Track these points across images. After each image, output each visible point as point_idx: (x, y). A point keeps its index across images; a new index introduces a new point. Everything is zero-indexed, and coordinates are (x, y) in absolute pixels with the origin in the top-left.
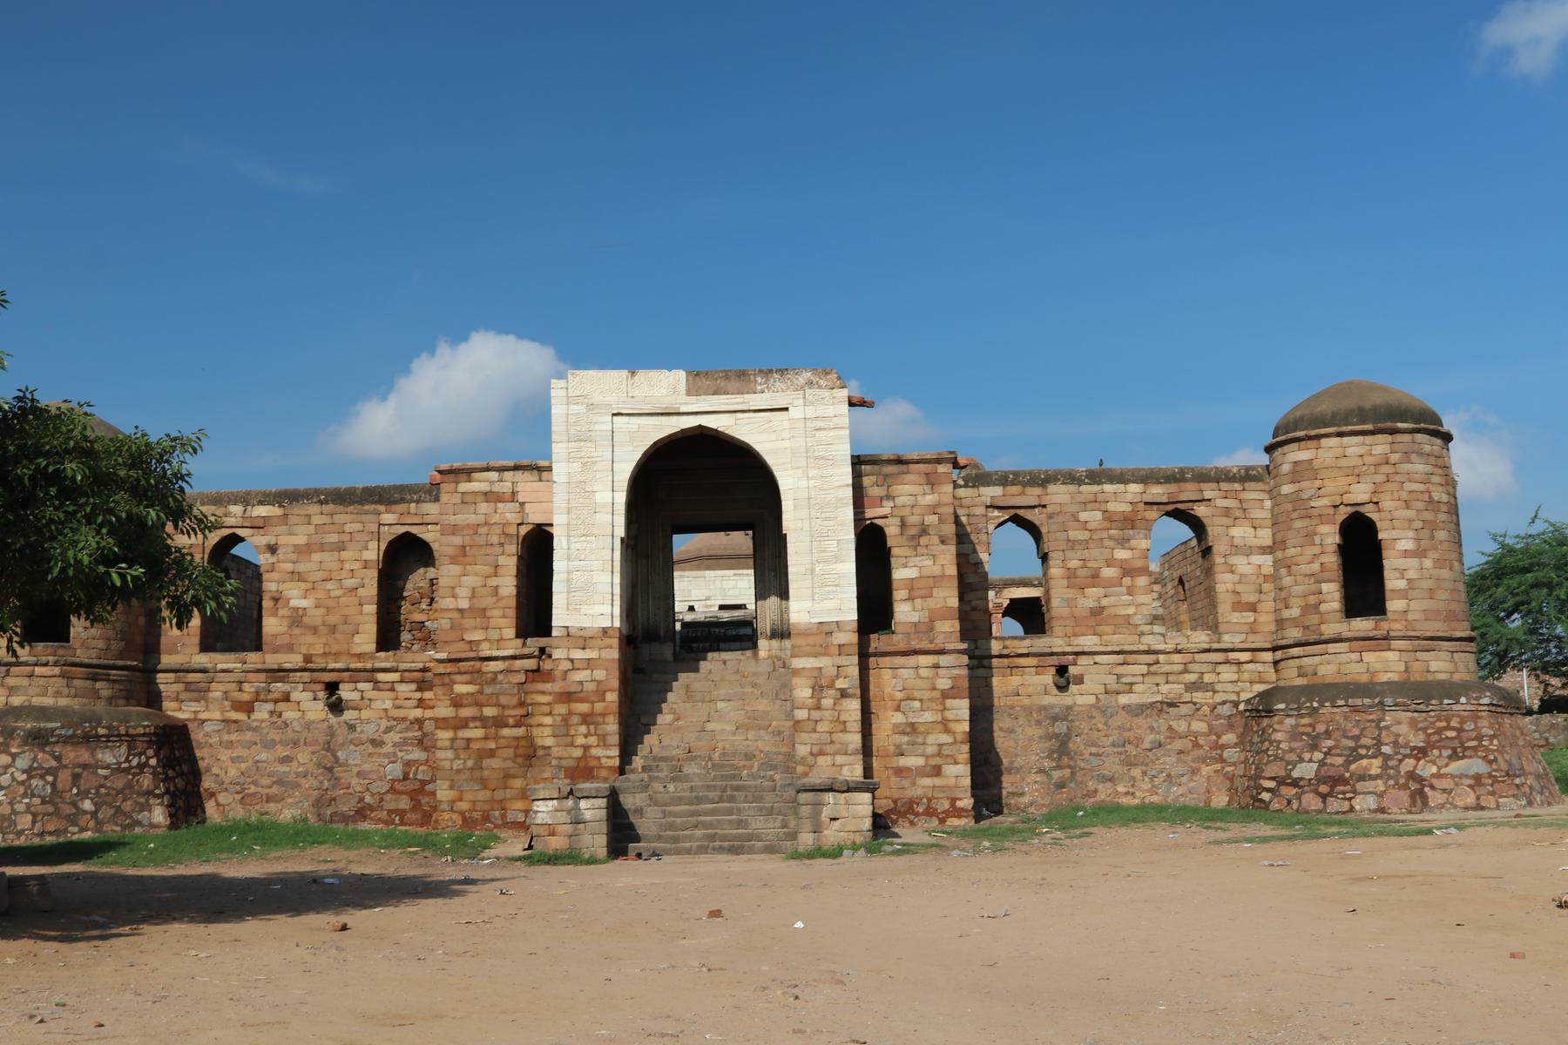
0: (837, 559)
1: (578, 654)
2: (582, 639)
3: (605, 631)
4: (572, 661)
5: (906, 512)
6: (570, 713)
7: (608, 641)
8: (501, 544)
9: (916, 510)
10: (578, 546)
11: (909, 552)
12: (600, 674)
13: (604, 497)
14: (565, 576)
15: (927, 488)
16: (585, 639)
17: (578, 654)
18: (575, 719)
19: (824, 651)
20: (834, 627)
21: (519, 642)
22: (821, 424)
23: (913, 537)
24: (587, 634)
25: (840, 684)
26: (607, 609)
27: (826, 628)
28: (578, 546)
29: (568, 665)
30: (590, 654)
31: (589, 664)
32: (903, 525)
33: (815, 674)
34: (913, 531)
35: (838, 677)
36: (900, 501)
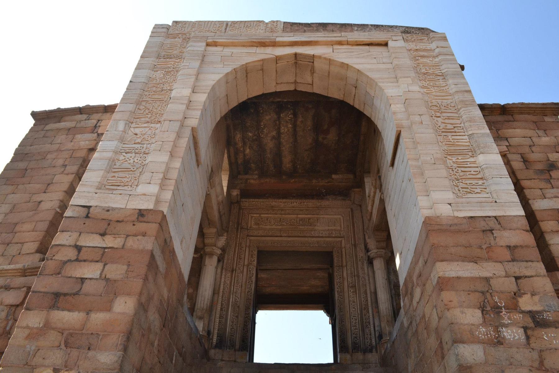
1: (92, 241)
2: (104, 222)
3: (141, 214)
4: (79, 248)
5: (526, 150)
6: (47, 326)
7: (141, 227)
8: (65, 166)
9: (534, 149)
10: (137, 131)
11: (542, 185)
12: (116, 271)
13: (181, 90)
14: (109, 155)
15: (541, 133)
17: (92, 241)
18: (53, 337)
19: (486, 254)
20: (492, 224)
21: (38, 256)
22: (426, 54)
23: (541, 171)
24: (114, 216)
25: (527, 303)
28: (137, 131)
29: (72, 254)
30: (109, 242)
31: (103, 256)
32: (525, 161)
33: (480, 286)
34: (540, 166)
35: (517, 294)
36: (514, 141)
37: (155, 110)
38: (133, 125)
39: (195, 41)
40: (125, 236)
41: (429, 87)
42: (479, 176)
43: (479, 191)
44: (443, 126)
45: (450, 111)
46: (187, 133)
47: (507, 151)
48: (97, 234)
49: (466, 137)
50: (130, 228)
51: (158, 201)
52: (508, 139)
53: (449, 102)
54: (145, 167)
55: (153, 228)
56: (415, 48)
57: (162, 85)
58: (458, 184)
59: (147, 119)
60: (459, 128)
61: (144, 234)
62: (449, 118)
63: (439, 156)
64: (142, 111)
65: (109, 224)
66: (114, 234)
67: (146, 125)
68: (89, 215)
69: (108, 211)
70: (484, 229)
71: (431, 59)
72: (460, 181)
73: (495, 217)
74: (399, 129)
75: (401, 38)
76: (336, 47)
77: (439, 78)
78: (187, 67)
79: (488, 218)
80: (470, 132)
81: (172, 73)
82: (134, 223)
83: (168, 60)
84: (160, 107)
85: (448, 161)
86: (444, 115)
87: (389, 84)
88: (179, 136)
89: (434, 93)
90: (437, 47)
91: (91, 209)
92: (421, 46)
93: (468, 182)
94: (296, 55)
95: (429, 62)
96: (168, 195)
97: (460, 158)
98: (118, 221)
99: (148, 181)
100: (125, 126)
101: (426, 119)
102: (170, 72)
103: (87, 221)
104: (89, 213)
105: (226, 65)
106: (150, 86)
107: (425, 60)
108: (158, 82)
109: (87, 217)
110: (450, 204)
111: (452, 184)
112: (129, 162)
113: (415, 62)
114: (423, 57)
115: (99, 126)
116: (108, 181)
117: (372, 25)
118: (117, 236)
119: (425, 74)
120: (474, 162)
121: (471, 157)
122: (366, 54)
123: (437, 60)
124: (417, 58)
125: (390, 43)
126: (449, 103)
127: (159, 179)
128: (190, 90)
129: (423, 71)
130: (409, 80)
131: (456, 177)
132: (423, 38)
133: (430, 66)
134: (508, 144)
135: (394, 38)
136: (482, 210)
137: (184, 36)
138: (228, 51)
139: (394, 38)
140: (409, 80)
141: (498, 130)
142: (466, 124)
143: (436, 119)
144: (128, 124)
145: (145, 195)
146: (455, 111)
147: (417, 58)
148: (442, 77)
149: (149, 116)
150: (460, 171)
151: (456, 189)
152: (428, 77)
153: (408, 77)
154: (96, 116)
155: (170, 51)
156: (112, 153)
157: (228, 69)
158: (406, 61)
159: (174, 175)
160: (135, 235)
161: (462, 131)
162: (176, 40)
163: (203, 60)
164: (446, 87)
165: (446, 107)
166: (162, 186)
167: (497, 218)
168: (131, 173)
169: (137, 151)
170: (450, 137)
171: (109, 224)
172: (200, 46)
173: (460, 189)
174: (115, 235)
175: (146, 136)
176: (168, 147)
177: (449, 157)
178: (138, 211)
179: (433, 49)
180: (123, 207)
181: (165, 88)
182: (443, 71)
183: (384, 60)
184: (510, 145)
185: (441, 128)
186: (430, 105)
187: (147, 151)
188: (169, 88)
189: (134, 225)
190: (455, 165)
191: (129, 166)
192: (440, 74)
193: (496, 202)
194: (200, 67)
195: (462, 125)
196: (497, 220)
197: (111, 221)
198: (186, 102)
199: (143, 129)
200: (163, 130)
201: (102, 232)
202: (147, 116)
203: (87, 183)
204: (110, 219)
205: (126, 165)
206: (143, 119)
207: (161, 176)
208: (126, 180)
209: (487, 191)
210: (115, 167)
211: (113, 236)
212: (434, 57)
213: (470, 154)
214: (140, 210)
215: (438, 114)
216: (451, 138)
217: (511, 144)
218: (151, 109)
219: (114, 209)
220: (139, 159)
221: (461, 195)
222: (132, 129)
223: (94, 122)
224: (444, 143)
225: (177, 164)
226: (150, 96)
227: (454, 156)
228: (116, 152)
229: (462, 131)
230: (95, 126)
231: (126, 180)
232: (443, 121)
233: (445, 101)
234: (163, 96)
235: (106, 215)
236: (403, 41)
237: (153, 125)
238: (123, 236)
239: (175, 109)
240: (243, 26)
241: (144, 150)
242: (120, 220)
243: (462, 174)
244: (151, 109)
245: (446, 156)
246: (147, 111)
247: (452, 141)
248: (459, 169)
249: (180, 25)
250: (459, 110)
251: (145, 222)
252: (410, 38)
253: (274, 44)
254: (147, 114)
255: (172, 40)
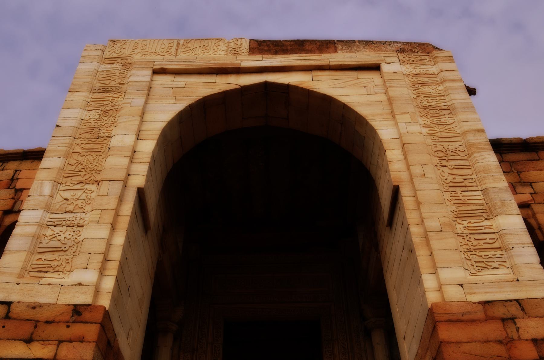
0: (489, 212)
3: (77, 310)
7: (78, 329)
10: (67, 195)
13: (122, 138)
14: (32, 230)
16: (36, 323)
20: (514, 310)
22: (427, 80)
24: (43, 315)
26: (90, 277)
27: (500, 312)
28: (67, 195)
37: (90, 166)
38: (62, 187)
39: (138, 69)
40: (57, 342)
41: (432, 125)
42: (497, 245)
43: (496, 265)
44: (450, 178)
45: (459, 157)
46: (131, 196)
47: (531, 201)
48: (20, 340)
49: (479, 193)
50: (63, 332)
51: (97, 292)
52: (533, 184)
53: (457, 144)
54: (79, 245)
55: (91, 331)
56: (414, 72)
57: (97, 130)
58: (471, 256)
59: (79, 178)
60: (470, 181)
61: (81, 340)
62: (457, 167)
63: (446, 220)
64: (74, 167)
65: (36, 327)
66: (43, 341)
67: (78, 187)
68: (10, 315)
69: (34, 308)
70: (505, 316)
71: (434, 87)
72: (473, 253)
73: (517, 301)
74: (396, 184)
75: (396, 59)
76: (316, 73)
77: (444, 112)
78: (129, 105)
79: (509, 303)
80: (484, 187)
81: (110, 112)
82: (68, 324)
83: (104, 94)
84: (96, 161)
85: (458, 226)
86: (453, 163)
87: (382, 122)
88: (121, 200)
89: (439, 134)
90: (442, 71)
91: (12, 306)
92: (421, 69)
93: (483, 253)
94: (266, 85)
95: (431, 91)
96: (109, 283)
97: (472, 221)
98: (47, 322)
99: (85, 266)
100: (52, 189)
101: (430, 171)
102: (106, 112)
103: (8, 323)
104: (9, 312)
105: (178, 100)
106: (82, 132)
107: (426, 89)
108: (92, 126)
109: (7, 317)
110: (461, 285)
111: (463, 256)
112: (59, 238)
113: (414, 92)
114: (424, 84)
115: (18, 179)
116: (33, 266)
117: (359, 42)
118: (47, 342)
119: (426, 107)
120: (489, 227)
121: (486, 219)
122: (352, 82)
123: (441, 88)
124: (417, 86)
125: (385, 68)
126: (457, 146)
127: (97, 262)
128: (134, 137)
129: (425, 103)
130: (407, 118)
131: (468, 247)
132: (423, 58)
133: (433, 96)
134: (532, 191)
135: (388, 60)
136: (500, 292)
137: (124, 61)
138: (180, 81)
139: (388, 60)
140: (407, 118)
141: (519, 173)
142: (479, 175)
143: (442, 168)
144: (57, 186)
145: (80, 284)
146: (465, 158)
147: (417, 86)
148: (449, 112)
149: (82, 174)
150: (472, 239)
151: (469, 263)
152: (431, 112)
153: (405, 113)
154: (12, 165)
155: (107, 82)
156: (36, 227)
157: (180, 107)
158: (402, 91)
159: (116, 254)
160: (70, 341)
161: (474, 184)
162: (114, 66)
163: (148, 94)
164: (454, 125)
165: (455, 152)
166: (102, 272)
167: (520, 301)
168: (62, 253)
169: (68, 223)
170: (459, 194)
171: (36, 327)
172: (144, 75)
173: (474, 263)
174: (44, 341)
175: (79, 202)
176: (108, 217)
177: (459, 221)
178: (72, 307)
179: (436, 73)
180: (53, 301)
181: (102, 135)
182: (449, 104)
183: (377, 90)
184: (535, 193)
185: (448, 181)
186: (435, 150)
187: (81, 223)
188: (107, 134)
189: (68, 326)
190: (467, 232)
191: (58, 244)
192: (446, 107)
193: (518, 280)
194: (146, 103)
195: (474, 176)
196: (520, 305)
197: (37, 321)
198: (129, 154)
199: (76, 192)
200: (101, 193)
201: (27, 336)
202: (80, 173)
203: (5, 270)
204: (36, 319)
205: (54, 243)
206: (74, 178)
207: (100, 258)
208: (56, 263)
209: (507, 264)
210: (41, 245)
211: (42, 342)
212: (437, 84)
213: (485, 215)
214: (75, 306)
215: (444, 163)
216: (461, 195)
217: (537, 190)
218: (85, 164)
219: (41, 306)
220: (72, 234)
221: (475, 272)
222: (62, 193)
223: (10, 173)
224: (452, 202)
225: (120, 239)
226: (83, 146)
227: (465, 219)
228: (41, 226)
229: (474, 184)
230: (12, 180)
231: (56, 263)
232: (451, 172)
233: (451, 144)
234: (99, 146)
235: (31, 314)
236: (398, 64)
237: (87, 187)
238: (54, 342)
239: (116, 163)
240: (198, 47)
241: (77, 221)
242: (50, 320)
243: (476, 243)
244: (85, 164)
245: (455, 219)
246: (80, 167)
247: (462, 198)
248: (471, 236)
249: (119, 45)
250: (470, 156)
251: (81, 322)
252: (407, 59)
253: (239, 71)
254: (80, 171)
255: (109, 66)
